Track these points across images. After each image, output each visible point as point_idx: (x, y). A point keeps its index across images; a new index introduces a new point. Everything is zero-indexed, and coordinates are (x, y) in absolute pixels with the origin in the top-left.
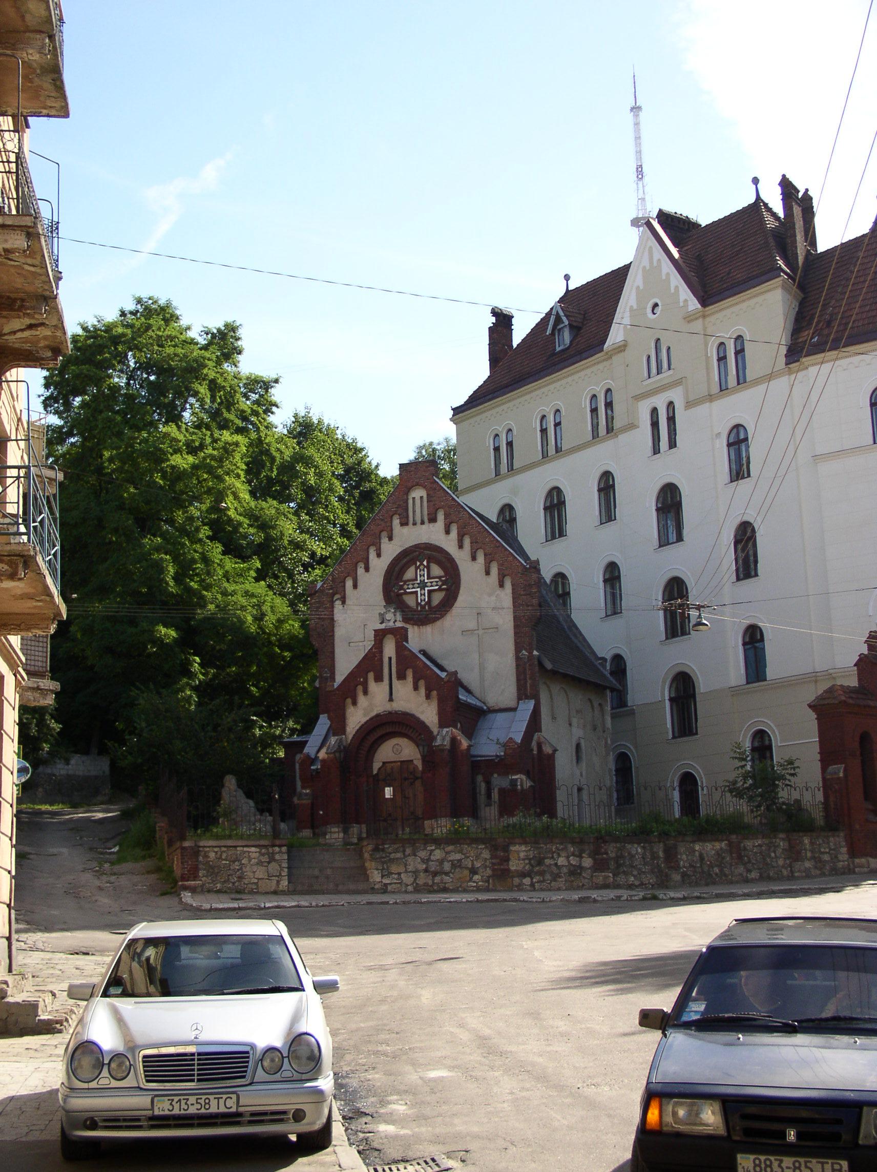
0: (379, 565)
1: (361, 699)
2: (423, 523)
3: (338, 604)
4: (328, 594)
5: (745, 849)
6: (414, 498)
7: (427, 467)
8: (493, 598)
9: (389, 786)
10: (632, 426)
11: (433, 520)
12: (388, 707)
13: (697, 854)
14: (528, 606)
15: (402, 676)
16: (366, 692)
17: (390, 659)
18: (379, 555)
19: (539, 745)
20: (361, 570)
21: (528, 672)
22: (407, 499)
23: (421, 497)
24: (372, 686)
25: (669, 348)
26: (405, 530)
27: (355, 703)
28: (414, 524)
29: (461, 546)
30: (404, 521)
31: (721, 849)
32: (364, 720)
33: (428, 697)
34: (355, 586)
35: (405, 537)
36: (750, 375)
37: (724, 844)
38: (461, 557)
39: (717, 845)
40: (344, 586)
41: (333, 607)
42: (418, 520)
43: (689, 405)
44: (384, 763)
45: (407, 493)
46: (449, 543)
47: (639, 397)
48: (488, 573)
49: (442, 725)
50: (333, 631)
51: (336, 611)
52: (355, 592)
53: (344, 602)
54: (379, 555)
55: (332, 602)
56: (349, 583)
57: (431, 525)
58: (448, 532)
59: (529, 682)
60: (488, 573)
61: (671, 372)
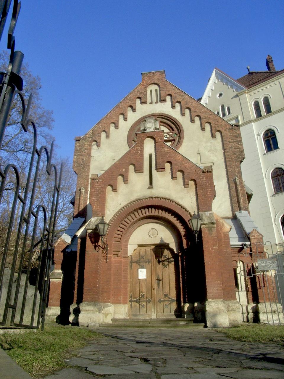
0: (125, 126)
1: (121, 186)
2: (157, 103)
3: (94, 147)
4: (88, 141)
6: (151, 91)
7: (161, 74)
8: (209, 144)
9: (142, 267)
11: (163, 100)
12: (148, 193)
14: (236, 149)
15: (160, 169)
16: (126, 181)
17: (150, 156)
18: (125, 119)
22: (146, 91)
23: (156, 90)
24: (132, 175)
25: (229, 109)
26: (144, 106)
27: (114, 189)
28: (151, 103)
29: (183, 114)
30: (143, 100)
32: (124, 204)
34: (108, 137)
36: (273, 109)
38: (184, 121)
40: (100, 136)
41: (90, 149)
42: (154, 100)
44: (140, 246)
45: (146, 87)
46: (175, 113)
48: (203, 129)
50: (90, 163)
51: (93, 151)
52: (108, 140)
53: (98, 145)
54: (125, 119)
55: (90, 145)
56: (103, 135)
57: (163, 104)
58: (173, 107)
60: (203, 129)
61: (230, 115)
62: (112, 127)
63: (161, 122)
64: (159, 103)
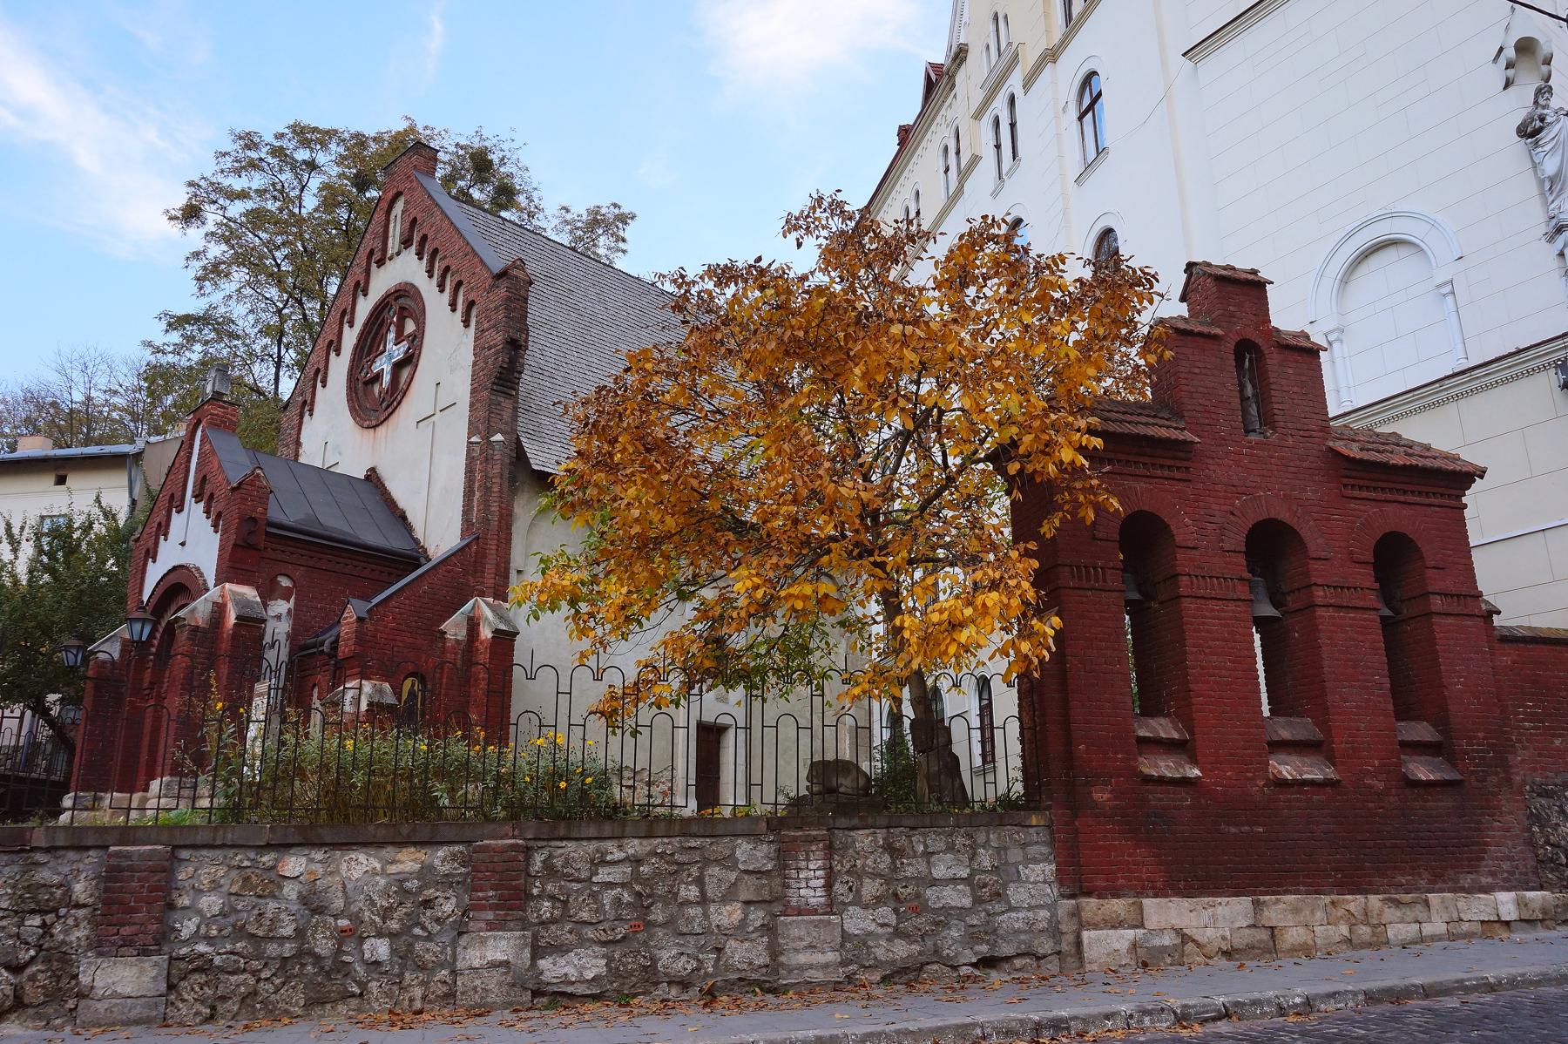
2: (398, 254)
5: (550, 870)
10: (975, 160)
13: (290, 891)
19: (473, 624)
20: (333, 354)
21: (478, 476)
29: (430, 273)
31: (426, 872)
33: (215, 526)
35: (382, 281)
37: (440, 858)
39: (408, 861)
43: (1028, 84)
47: (978, 115)
49: (218, 582)
54: (351, 324)
59: (477, 495)
62: (333, 354)
63: (402, 309)
64: (404, 253)
